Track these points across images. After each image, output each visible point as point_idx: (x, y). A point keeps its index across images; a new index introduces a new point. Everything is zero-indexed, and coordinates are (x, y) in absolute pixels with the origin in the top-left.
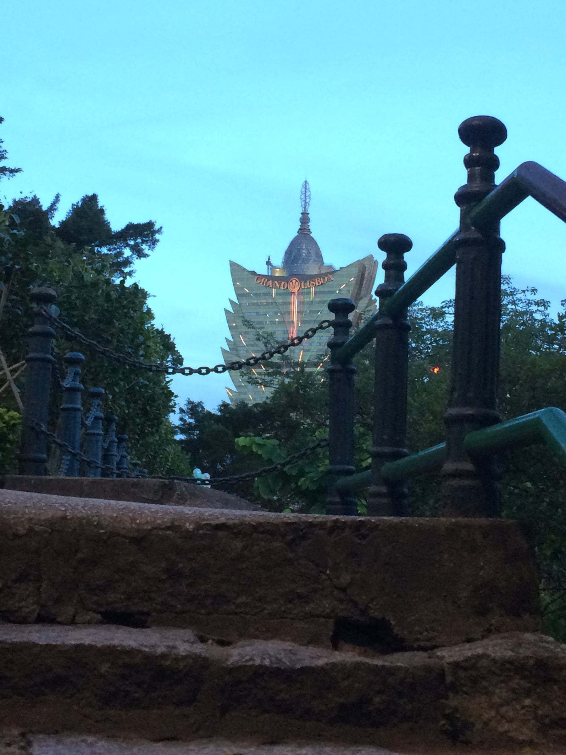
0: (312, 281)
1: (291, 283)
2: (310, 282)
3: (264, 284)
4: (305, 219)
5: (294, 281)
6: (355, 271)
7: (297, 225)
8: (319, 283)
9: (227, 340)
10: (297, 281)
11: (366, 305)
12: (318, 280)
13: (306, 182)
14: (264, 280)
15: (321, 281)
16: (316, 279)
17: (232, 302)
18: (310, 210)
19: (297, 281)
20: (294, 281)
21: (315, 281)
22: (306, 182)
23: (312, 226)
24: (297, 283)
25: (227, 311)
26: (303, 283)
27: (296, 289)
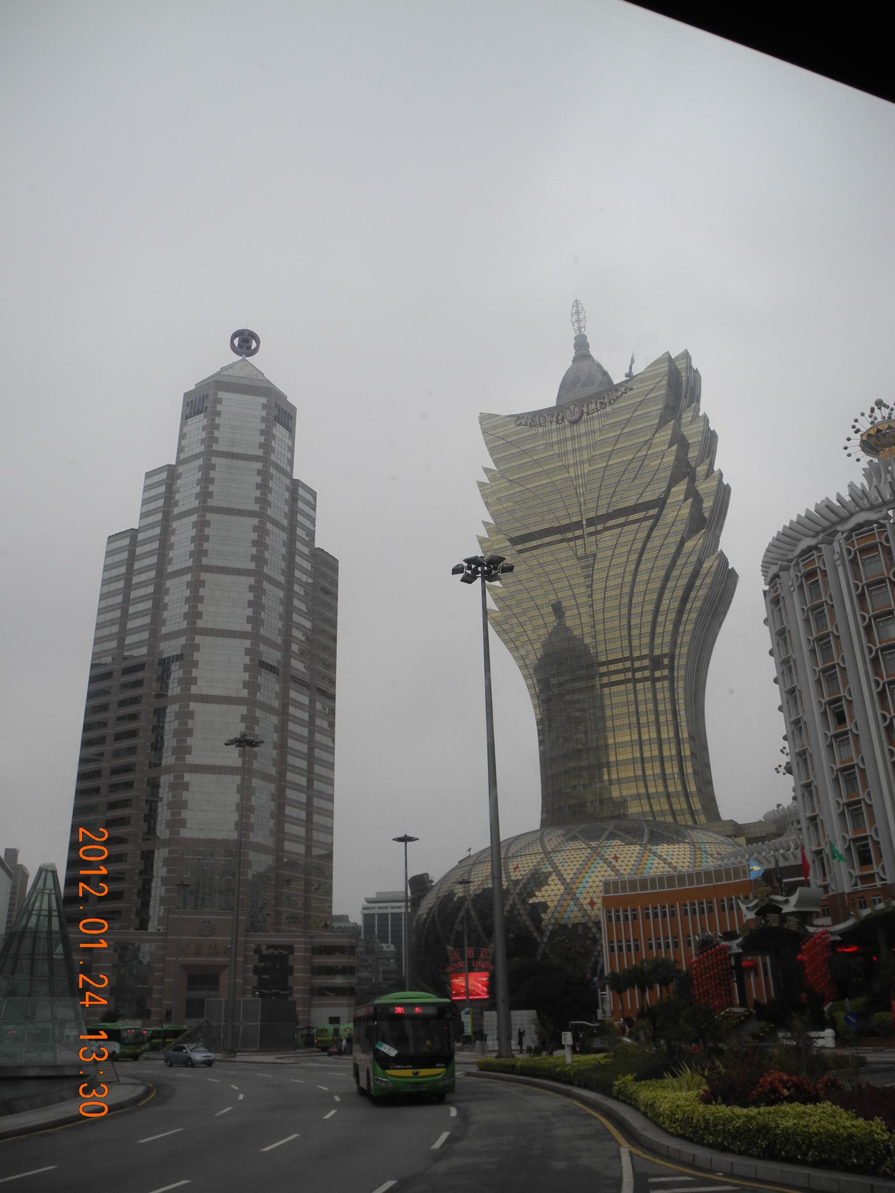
0: (600, 398)
1: (568, 410)
4: (581, 346)
5: (572, 407)
6: (664, 367)
7: (572, 353)
9: (486, 524)
11: (690, 419)
13: (577, 303)
16: (606, 395)
17: (487, 470)
18: (587, 332)
19: (576, 405)
20: (572, 407)
22: (577, 303)
23: (593, 352)
25: (481, 485)
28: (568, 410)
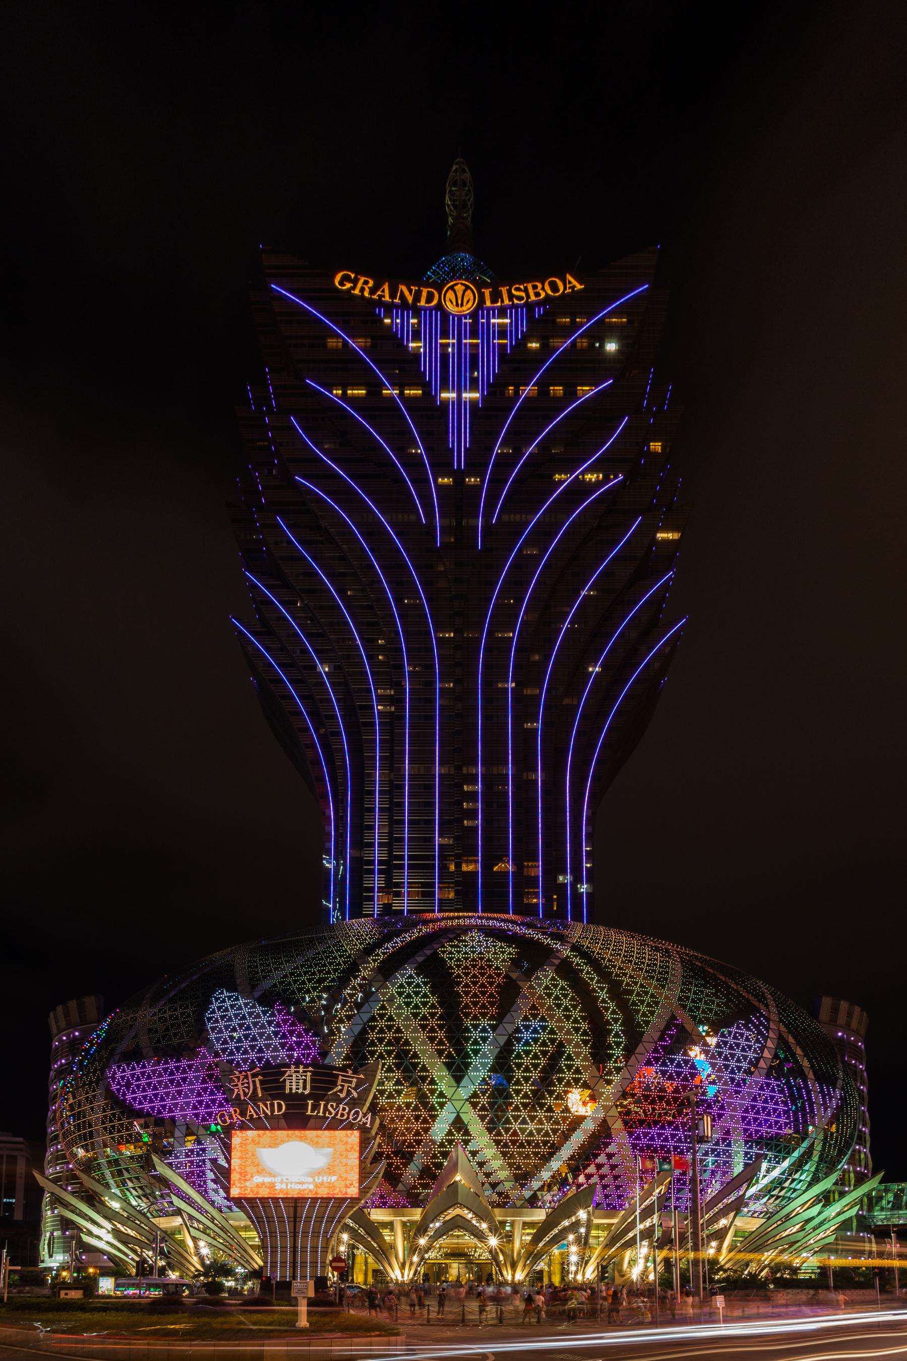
0: (518, 289)
1: (450, 292)
2: (509, 292)
3: (366, 294)
5: (459, 288)
8: (537, 294)
10: (467, 288)
12: (535, 287)
14: (366, 283)
15: (543, 289)
19: (467, 288)
20: (459, 288)
21: (526, 290)
24: (469, 291)
26: (487, 292)
27: (464, 308)
28: (450, 292)
